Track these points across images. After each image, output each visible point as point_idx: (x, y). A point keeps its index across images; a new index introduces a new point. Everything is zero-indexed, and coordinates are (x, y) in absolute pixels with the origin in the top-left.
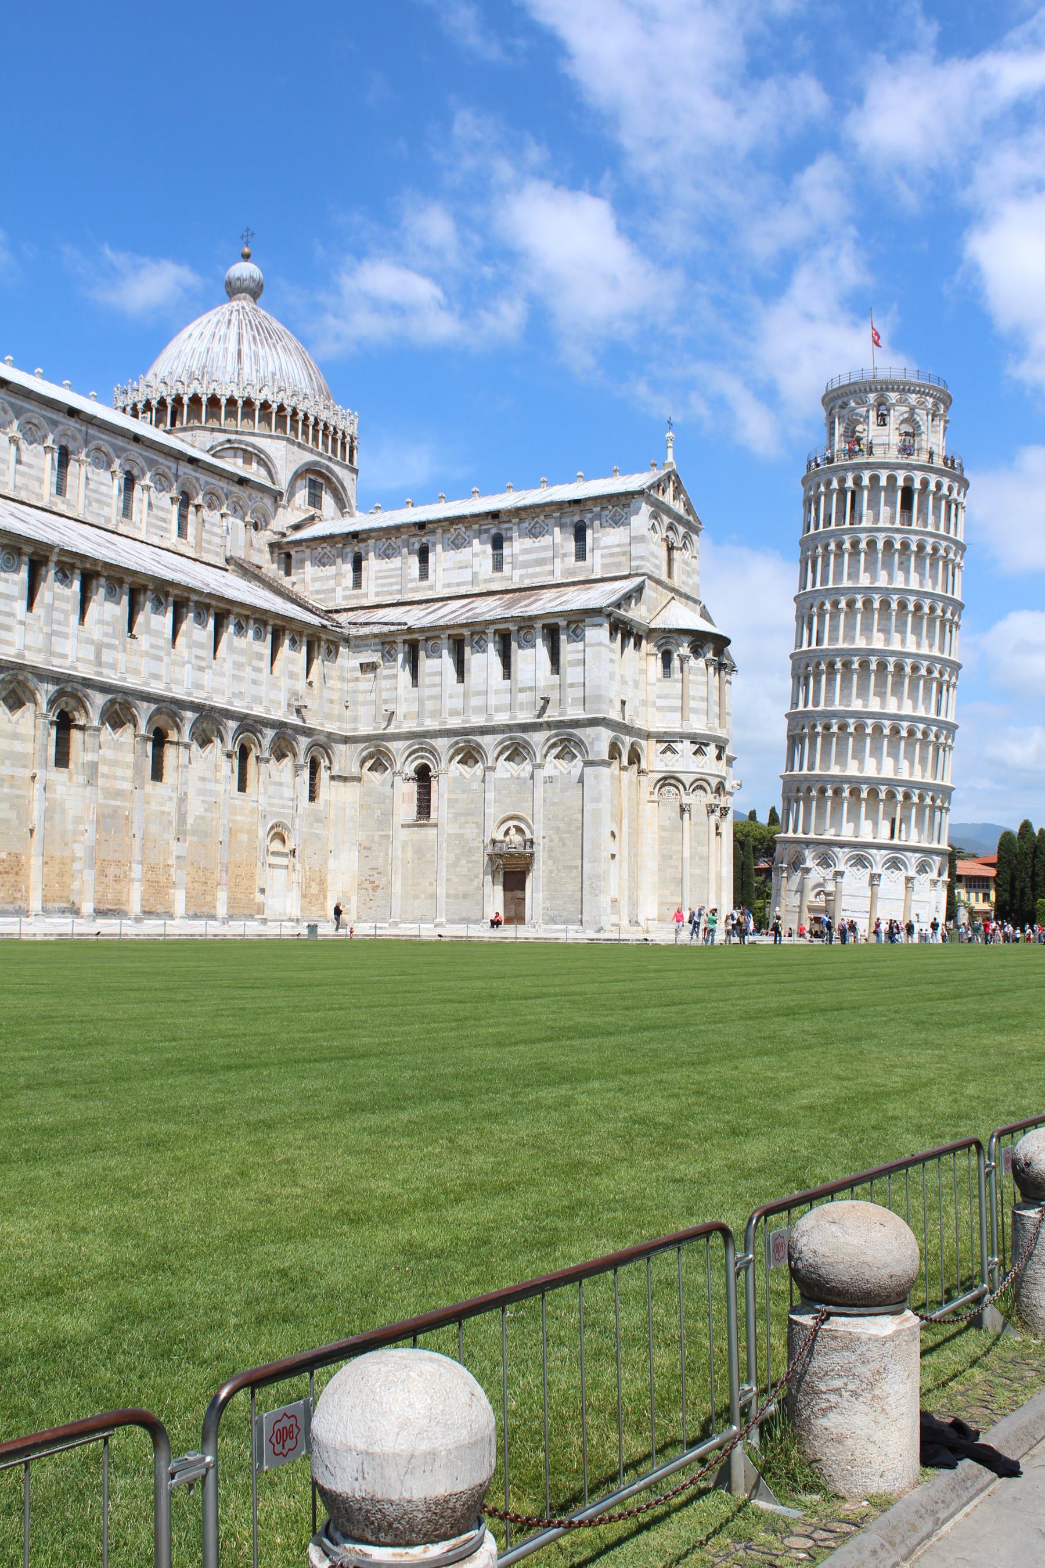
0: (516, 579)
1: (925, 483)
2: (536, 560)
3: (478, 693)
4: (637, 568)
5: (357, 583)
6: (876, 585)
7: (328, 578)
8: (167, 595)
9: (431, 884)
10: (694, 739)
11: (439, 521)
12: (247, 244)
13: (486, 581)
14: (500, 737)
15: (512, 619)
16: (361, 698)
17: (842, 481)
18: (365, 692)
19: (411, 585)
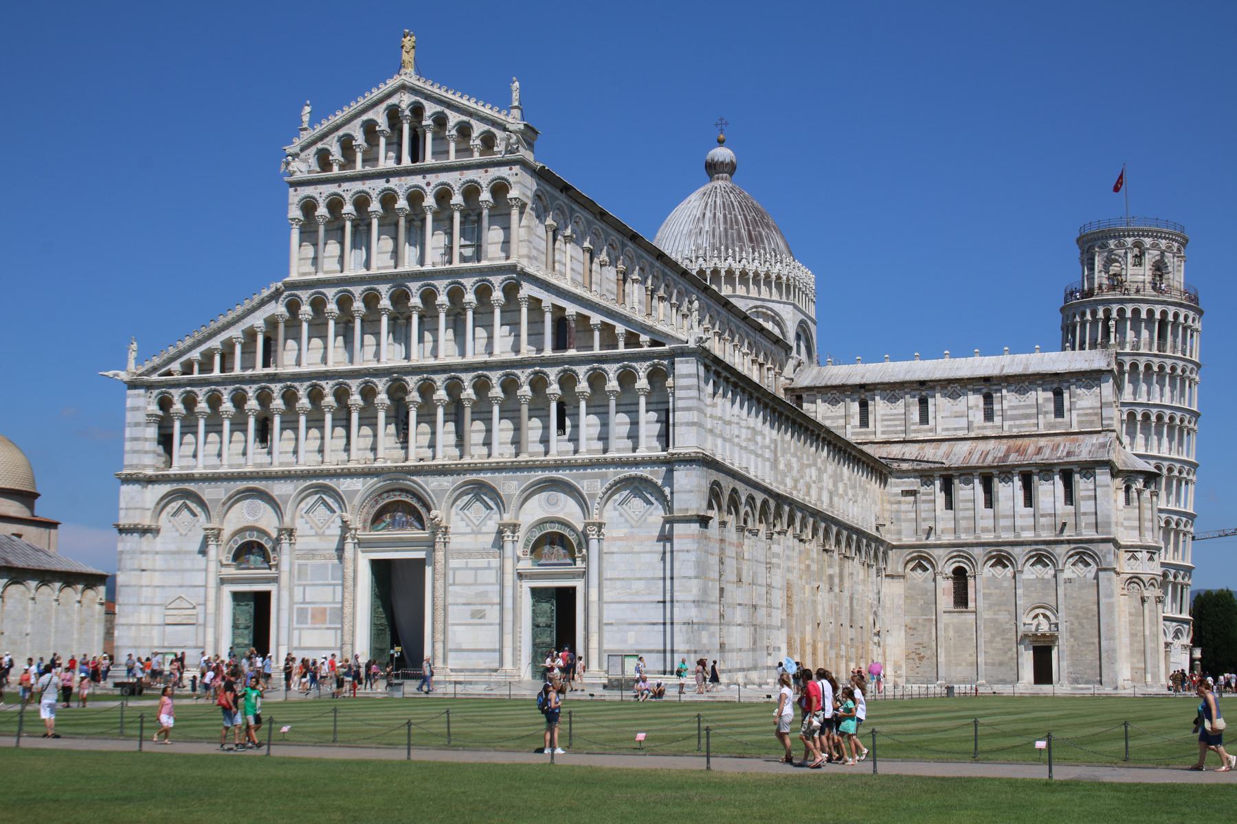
0: (1006, 428)
1: (1176, 315)
2: (1022, 415)
3: (1005, 517)
4: (1108, 425)
5: (864, 422)
6: (1139, 401)
7: (840, 417)
8: (845, 452)
9: (971, 655)
10: (1147, 548)
11: (939, 381)
12: (722, 131)
13: (979, 428)
14: (1028, 548)
15: (1036, 465)
16: (903, 516)
17: (1107, 313)
18: (906, 512)
19: (913, 427)
